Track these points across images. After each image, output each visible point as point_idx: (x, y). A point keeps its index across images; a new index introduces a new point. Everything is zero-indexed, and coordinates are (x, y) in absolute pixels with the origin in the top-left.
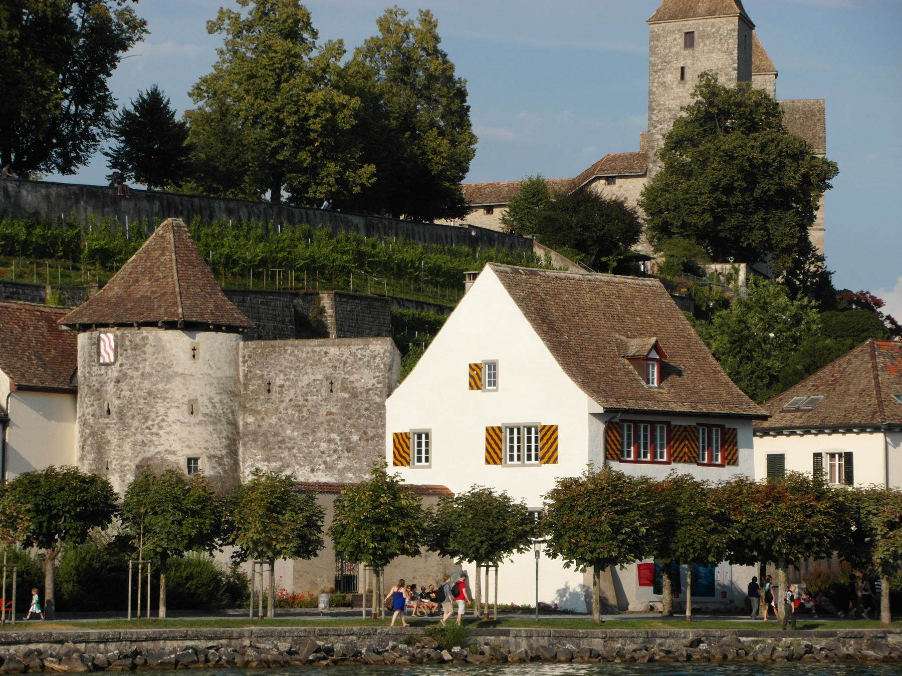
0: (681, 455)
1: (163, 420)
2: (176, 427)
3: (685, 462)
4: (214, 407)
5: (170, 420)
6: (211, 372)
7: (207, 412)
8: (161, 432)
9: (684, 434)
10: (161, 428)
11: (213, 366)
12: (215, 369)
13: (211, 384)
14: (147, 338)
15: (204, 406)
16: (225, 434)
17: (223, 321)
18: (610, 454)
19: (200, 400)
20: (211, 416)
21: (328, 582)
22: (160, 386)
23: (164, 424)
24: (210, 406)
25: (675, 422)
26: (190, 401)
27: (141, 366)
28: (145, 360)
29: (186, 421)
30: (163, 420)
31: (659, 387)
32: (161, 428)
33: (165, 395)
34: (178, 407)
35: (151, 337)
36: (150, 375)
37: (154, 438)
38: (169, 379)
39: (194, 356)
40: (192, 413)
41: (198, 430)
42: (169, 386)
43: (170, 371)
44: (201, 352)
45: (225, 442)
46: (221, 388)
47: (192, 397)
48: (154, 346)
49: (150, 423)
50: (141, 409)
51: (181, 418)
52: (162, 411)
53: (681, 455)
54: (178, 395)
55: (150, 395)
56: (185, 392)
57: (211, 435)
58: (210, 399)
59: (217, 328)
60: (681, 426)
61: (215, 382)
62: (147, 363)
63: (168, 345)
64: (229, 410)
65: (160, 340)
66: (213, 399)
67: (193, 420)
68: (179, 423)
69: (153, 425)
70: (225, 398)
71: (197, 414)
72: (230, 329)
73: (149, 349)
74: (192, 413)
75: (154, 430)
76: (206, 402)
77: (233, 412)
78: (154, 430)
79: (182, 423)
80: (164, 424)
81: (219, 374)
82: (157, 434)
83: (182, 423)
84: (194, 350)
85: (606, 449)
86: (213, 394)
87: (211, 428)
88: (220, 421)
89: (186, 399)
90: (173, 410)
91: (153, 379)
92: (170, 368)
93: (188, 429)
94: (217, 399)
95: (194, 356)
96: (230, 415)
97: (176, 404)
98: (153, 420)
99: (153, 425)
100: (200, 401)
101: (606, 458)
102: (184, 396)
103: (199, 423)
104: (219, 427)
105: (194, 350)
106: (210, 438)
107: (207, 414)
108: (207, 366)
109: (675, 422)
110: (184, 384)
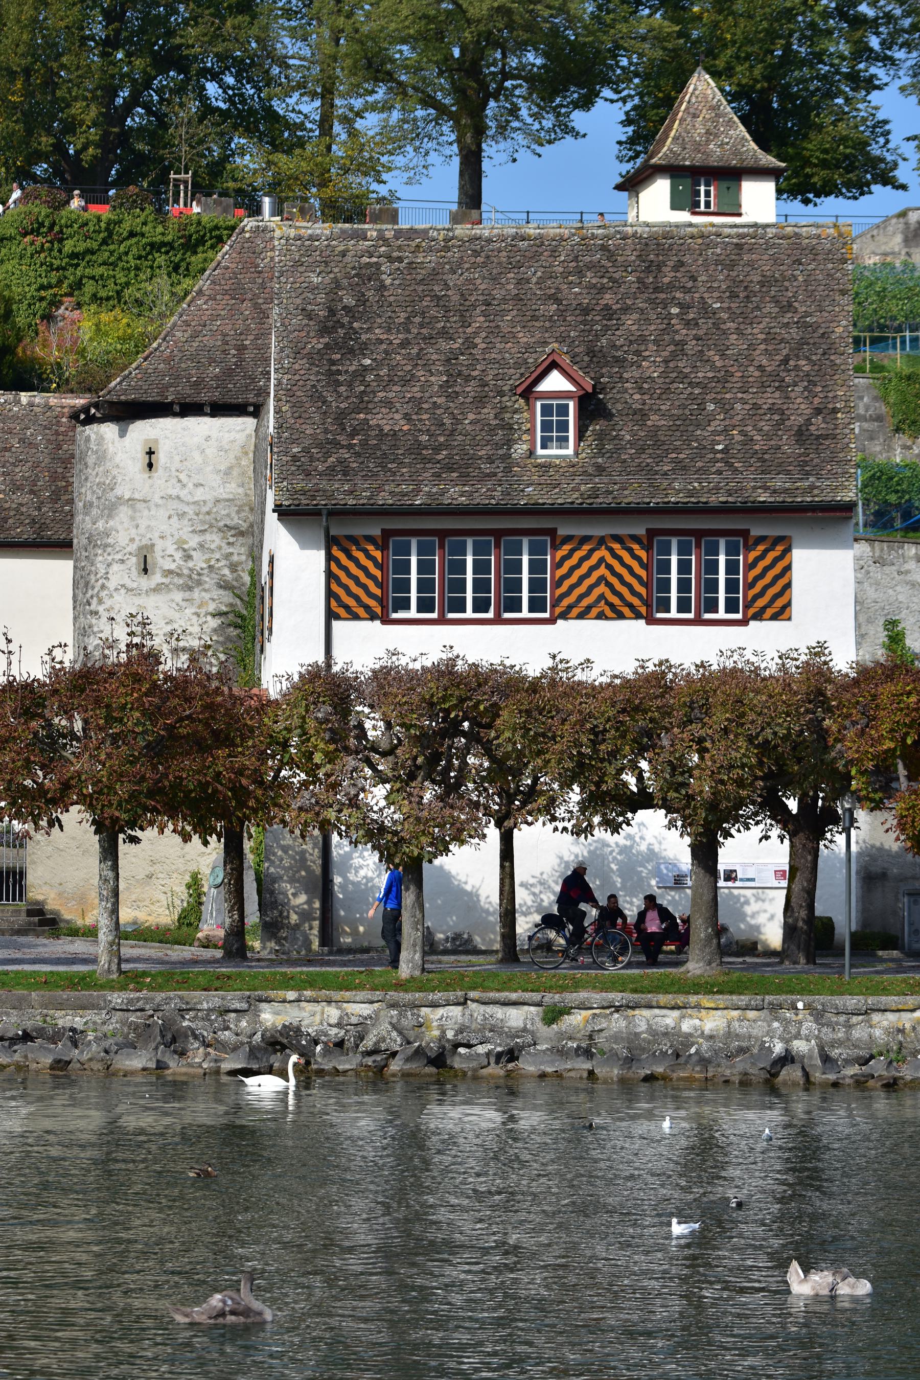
0: (585, 602)
1: (103, 587)
3: (601, 616)
4: (188, 557)
5: (112, 585)
6: (183, 494)
7: (173, 566)
8: (101, 609)
10: (100, 602)
12: (190, 485)
13: (181, 515)
14: (88, 439)
16: (212, 607)
17: (204, 397)
18: (347, 608)
19: (159, 545)
23: (103, 594)
24: (178, 555)
26: (140, 549)
27: (83, 490)
28: (86, 479)
29: (135, 585)
31: (577, 454)
32: (100, 602)
34: (122, 561)
36: (91, 504)
37: (94, 621)
38: (110, 510)
39: (150, 465)
40: (145, 570)
42: (111, 523)
43: (111, 496)
44: (161, 458)
45: (213, 623)
46: (203, 522)
47: (144, 542)
48: (97, 452)
49: (90, 593)
50: (83, 567)
53: (585, 602)
55: (90, 542)
56: (133, 531)
58: (180, 545)
59: (189, 409)
60: (585, 539)
61: (190, 510)
62: (89, 484)
63: (111, 450)
65: (101, 439)
67: (145, 583)
68: (123, 591)
69: (92, 597)
70: (214, 539)
71: (153, 574)
72: (220, 409)
73: (91, 459)
74: (145, 570)
76: (171, 549)
77: (233, 567)
78: (93, 607)
79: (128, 590)
80: (103, 594)
81: (199, 495)
82: (96, 613)
83: (128, 590)
84: (150, 453)
86: (185, 533)
87: (178, 596)
88: (199, 583)
89: (133, 548)
90: (115, 567)
91: (94, 511)
92: (112, 489)
94: (193, 542)
95: (150, 465)
96: (226, 571)
97: (118, 556)
98: (93, 588)
99: (92, 597)
100: (158, 549)
101: (330, 616)
102: (132, 540)
103: (157, 589)
104: (196, 594)
106: (177, 615)
107: (170, 572)
108: (174, 481)
110: (132, 518)
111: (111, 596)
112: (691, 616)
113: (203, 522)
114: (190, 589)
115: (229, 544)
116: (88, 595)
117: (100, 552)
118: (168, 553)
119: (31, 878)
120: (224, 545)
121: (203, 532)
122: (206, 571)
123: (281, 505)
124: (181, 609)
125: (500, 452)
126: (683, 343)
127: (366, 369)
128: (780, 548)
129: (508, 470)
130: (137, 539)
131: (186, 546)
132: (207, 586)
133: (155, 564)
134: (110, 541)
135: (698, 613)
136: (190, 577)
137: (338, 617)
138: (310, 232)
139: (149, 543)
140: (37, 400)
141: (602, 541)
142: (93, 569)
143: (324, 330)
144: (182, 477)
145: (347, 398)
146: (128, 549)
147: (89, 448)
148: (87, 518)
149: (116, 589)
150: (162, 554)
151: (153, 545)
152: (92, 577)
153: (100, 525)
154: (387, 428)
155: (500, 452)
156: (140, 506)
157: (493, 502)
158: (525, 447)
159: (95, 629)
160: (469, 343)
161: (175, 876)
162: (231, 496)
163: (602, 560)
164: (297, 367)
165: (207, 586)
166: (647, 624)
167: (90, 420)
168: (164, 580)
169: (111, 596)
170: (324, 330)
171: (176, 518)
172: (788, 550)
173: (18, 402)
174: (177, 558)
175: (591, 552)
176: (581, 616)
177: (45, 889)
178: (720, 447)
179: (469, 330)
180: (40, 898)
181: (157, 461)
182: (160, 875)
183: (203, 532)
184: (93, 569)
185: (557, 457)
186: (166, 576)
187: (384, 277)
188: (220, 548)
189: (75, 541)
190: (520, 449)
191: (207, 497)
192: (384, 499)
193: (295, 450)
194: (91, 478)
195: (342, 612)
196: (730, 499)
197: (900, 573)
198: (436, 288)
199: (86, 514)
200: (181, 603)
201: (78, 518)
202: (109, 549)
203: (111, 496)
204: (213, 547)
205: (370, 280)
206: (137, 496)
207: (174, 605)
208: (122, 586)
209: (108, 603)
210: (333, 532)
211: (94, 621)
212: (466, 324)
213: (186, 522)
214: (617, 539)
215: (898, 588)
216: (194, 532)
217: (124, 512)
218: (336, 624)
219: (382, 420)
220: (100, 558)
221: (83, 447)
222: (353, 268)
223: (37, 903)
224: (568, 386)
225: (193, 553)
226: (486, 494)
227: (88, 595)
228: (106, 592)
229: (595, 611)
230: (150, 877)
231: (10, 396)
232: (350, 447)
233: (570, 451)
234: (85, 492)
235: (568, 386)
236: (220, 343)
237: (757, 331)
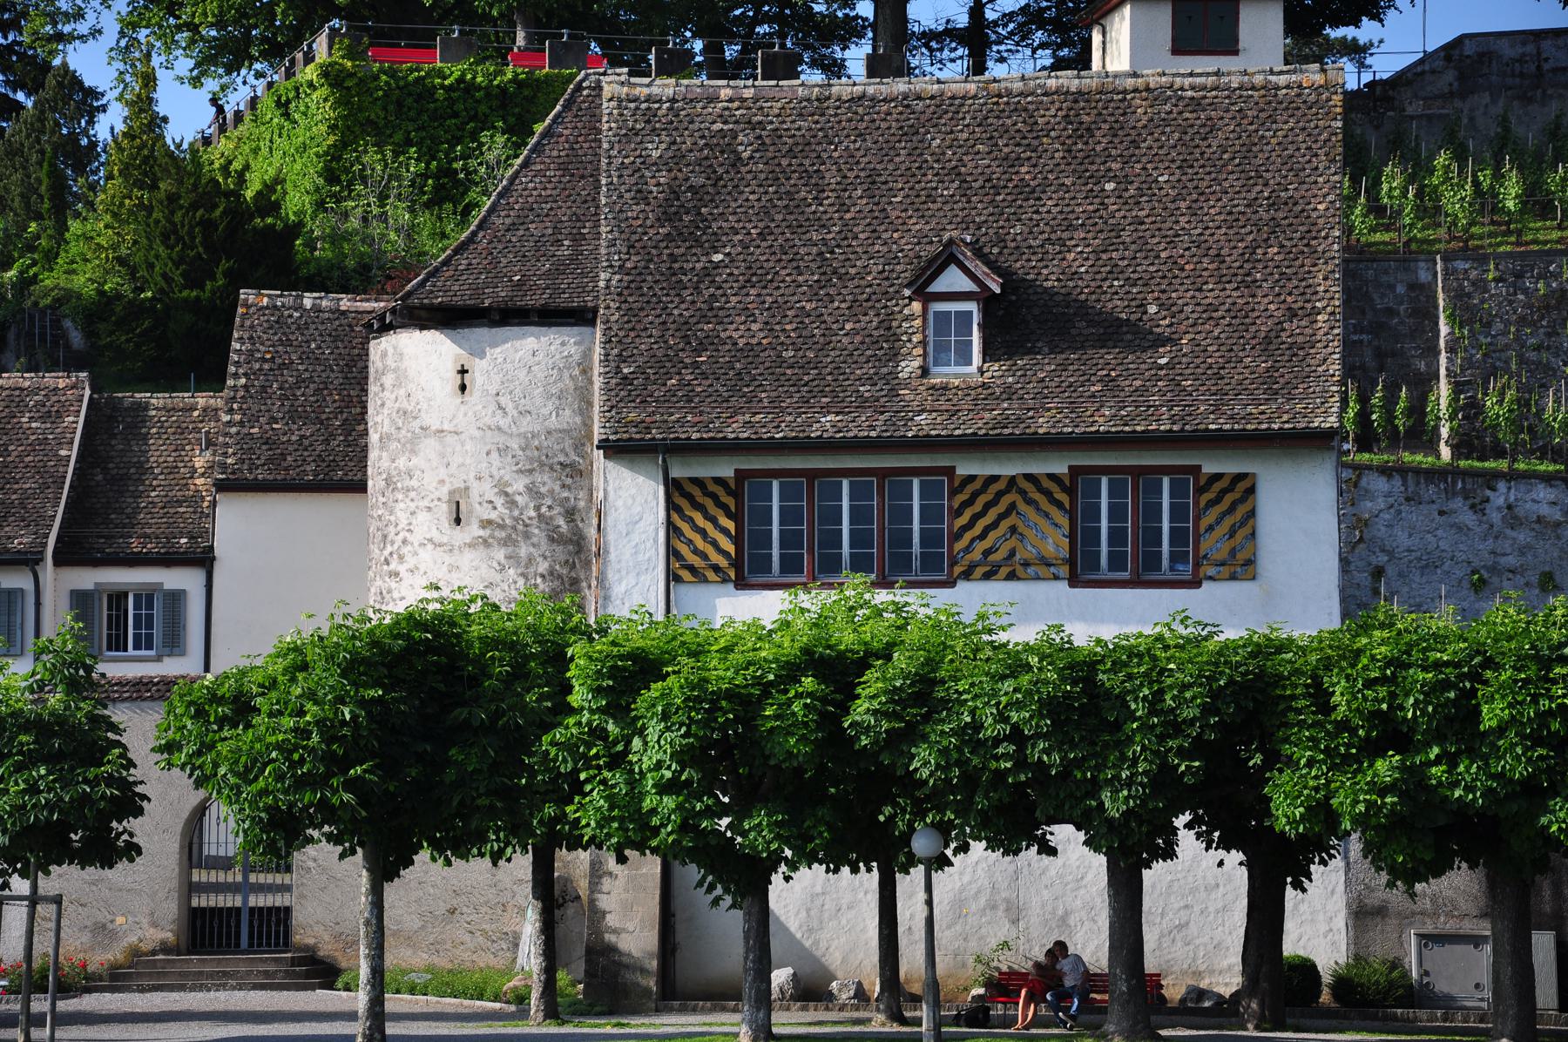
2: (426, 555)
5: (415, 539)
6: (504, 423)
7: (493, 516)
8: (402, 569)
9: (1006, 501)
11: (510, 407)
13: (503, 451)
14: (384, 355)
15: (483, 503)
16: (543, 567)
19: (476, 489)
20: (502, 527)
21: (154, 925)
22: (402, 463)
23: (405, 550)
24: (499, 502)
25: (966, 467)
28: (383, 405)
29: (445, 540)
30: (404, 542)
31: (981, 372)
32: (401, 558)
33: (408, 483)
35: (391, 351)
37: (393, 585)
38: (411, 446)
39: (463, 388)
40: (458, 521)
41: (468, 559)
42: (415, 461)
44: (477, 378)
46: (531, 460)
48: (395, 371)
49: (389, 549)
51: (435, 534)
52: (403, 518)
54: (430, 481)
57: (502, 569)
61: (514, 444)
62: (386, 411)
64: (557, 510)
66: (507, 484)
68: (430, 547)
70: (547, 482)
72: (550, 316)
74: (458, 521)
75: (393, 566)
76: (491, 494)
78: (393, 566)
80: (405, 550)
81: (527, 425)
82: (397, 574)
85: (672, 553)
87: (500, 554)
88: (527, 536)
89: (445, 490)
90: (422, 516)
91: (394, 445)
93: (448, 559)
94: (518, 485)
95: (463, 388)
96: (561, 522)
97: (423, 504)
98: (393, 543)
101: (672, 578)
102: (442, 482)
105: (463, 372)
106: (498, 577)
107: (490, 522)
108: (493, 407)
109: (966, 467)
111: (416, 554)
112: (1125, 575)
113: (531, 460)
114: (515, 543)
115: (563, 486)
116: (386, 553)
117: (400, 497)
118: (487, 498)
119: (298, 918)
120: (557, 488)
121: (531, 471)
122: (535, 522)
123: (607, 440)
124: (502, 569)
125: (884, 370)
126: (1117, 230)
127: (717, 266)
128: (1242, 486)
129: (893, 393)
130: (447, 480)
131: (509, 490)
132: (535, 540)
133: (471, 512)
134: (414, 483)
135: (1135, 571)
136: (514, 528)
137: (678, 579)
138: (646, 91)
139: (462, 486)
140: (324, 303)
141: (1012, 480)
142: (392, 518)
143: (666, 217)
144: (503, 400)
145: (693, 302)
146: (437, 494)
147: (385, 367)
148: (384, 454)
149: (422, 545)
150: (478, 499)
151: (467, 488)
152: (391, 529)
153: (402, 463)
154: (741, 342)
155: (884, 370)
156: (450, 439)
157: (873, 434)
158: (916, 364)
159: (396, 595)
160: (847, 232)
161: (483, 910)
162: (565, 426)
163: (1012, 506)
164: (628, 265)
165: (535, 540)
166: (1071, 586)
167: (385, 328)
168: (481, 533)
169: (416, 554)
170: (666, 217)
171: (495, 455)
172: (1251, 490)
173: (300, 307)
174: (499, 506)
175: (999, 495)
176: (987, 576)
177: (319, 929)
178: (1163, 361)
179: (848, 216)
180: (311, 941)
181: (473, 380)
182: (465, 909)
183: (531, 471)
184: (392, 518)
185: (956, 376)
186: (484, 528)
187: (741, 148)
188: (552, 492)
189: (370, 483)
190: (909, 367)
191: (537, 428)
192: (736, 430)
193: (625, 371)
194: (389, 404)
195: (686, 575)
196: (1175, 428)
197: (1441, 513)
198: (807, 162)
199: (381, 449)
200: (503, 561)
201: (373, 455)
202: (412, 494)
203: (416, 424)
204: (543, 490)
205: (722, 152)
206: (446, 427)
207: (495, 564)
208: (430, 540)
209: (411, 561)
210: (676, 473)
211: (393, 585)
212: (843, 208)
213: (509, 458)
214: (1029, 477)
215: (1440, 533)
216: (521, 471)
217: (429, 446)
218: (679, 591)
219: (735, 332)
220: (402, 505)
221: (379, 364)
222: (703, 137)
223: (307, 948)
224: (967, 285)
225: (518, 498)
226: (865, 426)
227: (386, 553)
228: (409, 548)
229: (1004, 571)
230: (452, 911)
231: (286, 299)
232: (696, 365)
233: (973, 368)
234: (380, 419)
235: (967, 285)
236: (550, 231)
237: (1213, 210)
